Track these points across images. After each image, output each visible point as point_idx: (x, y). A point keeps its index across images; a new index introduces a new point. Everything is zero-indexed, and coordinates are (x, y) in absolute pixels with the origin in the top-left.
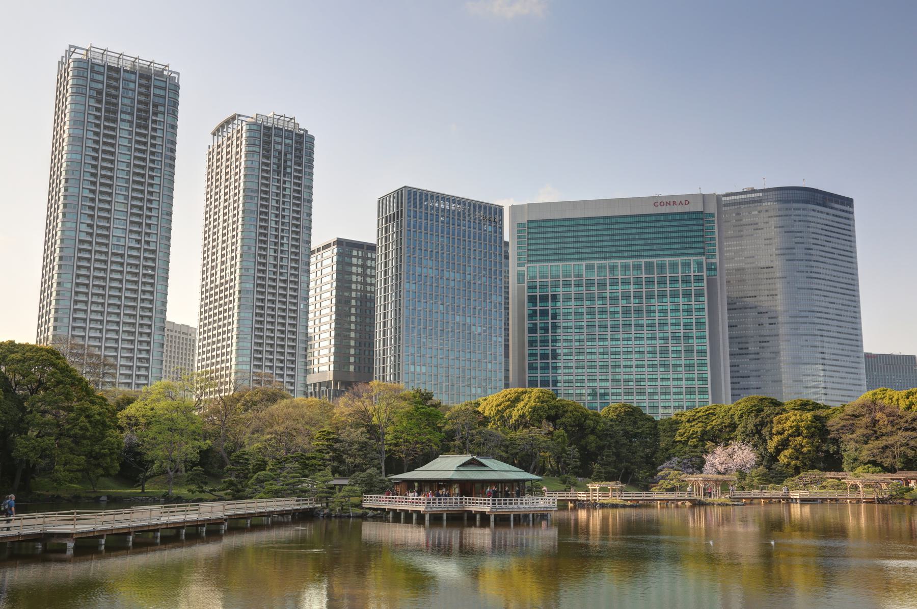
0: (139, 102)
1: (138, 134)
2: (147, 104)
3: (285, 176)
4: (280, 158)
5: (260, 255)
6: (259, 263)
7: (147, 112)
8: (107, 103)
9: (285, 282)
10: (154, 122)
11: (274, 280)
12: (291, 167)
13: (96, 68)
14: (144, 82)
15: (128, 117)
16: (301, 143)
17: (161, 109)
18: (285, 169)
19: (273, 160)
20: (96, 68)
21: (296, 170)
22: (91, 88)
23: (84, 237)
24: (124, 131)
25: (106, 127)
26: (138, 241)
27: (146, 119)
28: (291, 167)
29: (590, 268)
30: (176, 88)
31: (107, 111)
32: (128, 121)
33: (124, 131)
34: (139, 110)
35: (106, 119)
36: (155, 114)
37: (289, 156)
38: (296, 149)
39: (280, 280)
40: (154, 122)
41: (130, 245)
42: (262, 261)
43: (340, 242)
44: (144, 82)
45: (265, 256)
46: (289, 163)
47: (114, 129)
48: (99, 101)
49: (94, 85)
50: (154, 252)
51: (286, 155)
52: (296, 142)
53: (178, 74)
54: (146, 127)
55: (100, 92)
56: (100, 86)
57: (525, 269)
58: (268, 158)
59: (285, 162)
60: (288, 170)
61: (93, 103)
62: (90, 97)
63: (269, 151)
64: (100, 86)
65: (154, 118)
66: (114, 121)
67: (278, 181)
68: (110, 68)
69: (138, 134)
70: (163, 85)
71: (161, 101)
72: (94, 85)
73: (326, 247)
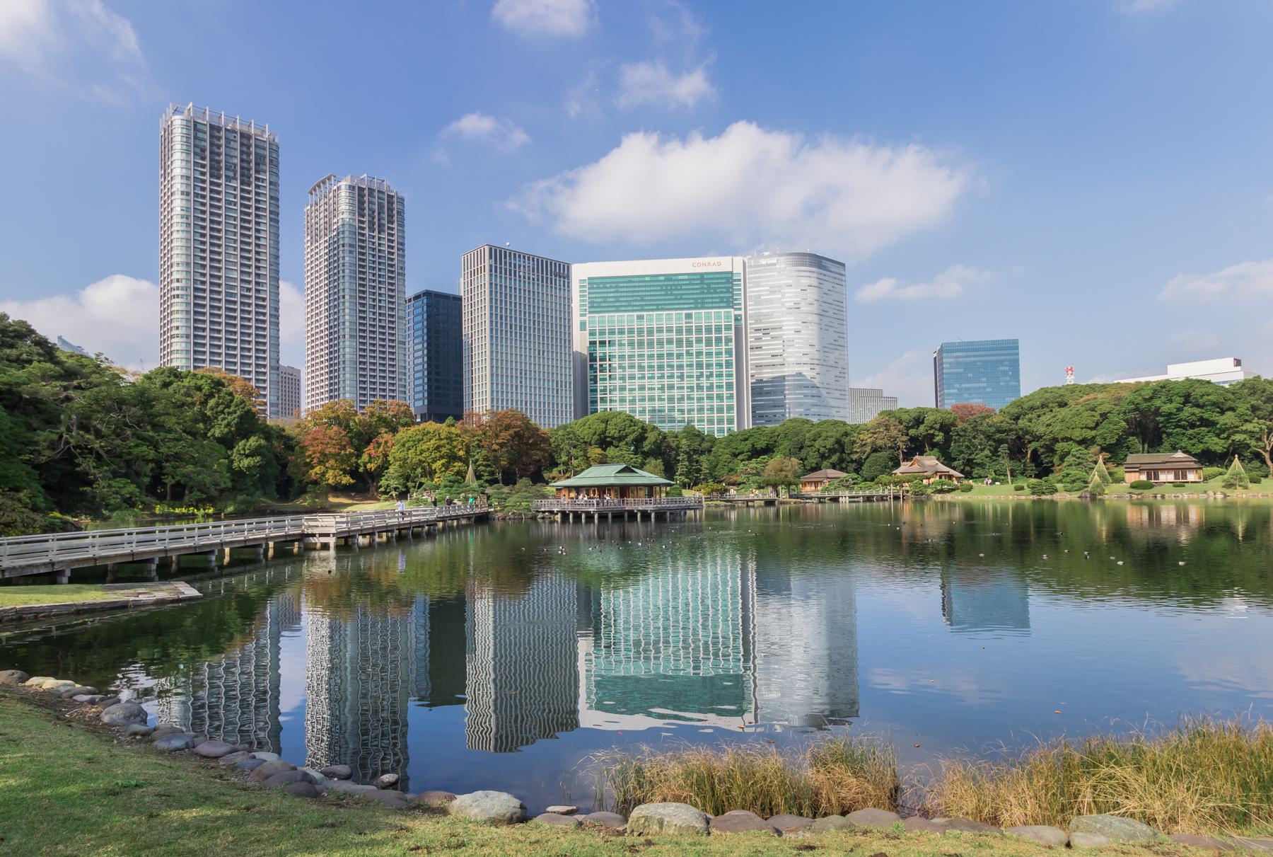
7: (249, 170)
8: (211, 160)
9: (383, 327)
11: (374, 326)
19: (366, 219)
20: (199, 127)
24: (230, 188)
30: (274, 148)
31: (211, 168)
40: (257, 179)
43: (428, 294)
44: (245, 141)
45: (363, 305)
48: (203, 158)
49: (198, 142)
50: (264, 300)
54: (249, 185)
56: (203, 143)
57: (586, 318)
64: (203, 143)
68: (212, 127)
72: (198, 142)
73: (417, 297)
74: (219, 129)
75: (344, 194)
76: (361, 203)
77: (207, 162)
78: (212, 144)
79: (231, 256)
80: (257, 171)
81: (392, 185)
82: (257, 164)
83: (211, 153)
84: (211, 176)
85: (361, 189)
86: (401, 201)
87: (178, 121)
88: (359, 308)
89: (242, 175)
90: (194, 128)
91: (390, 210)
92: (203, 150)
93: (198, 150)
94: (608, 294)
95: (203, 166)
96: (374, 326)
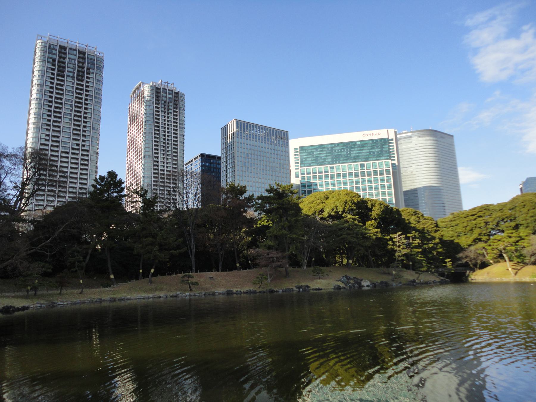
0: (79, 67)
1: (77, 84)
2: (83, 68)
3: (168, 114)
4: (166, 106)
5: (155, 157)
6: (155, 161)
7: (83, 72)
8: (59, 66)
10: (88, 78)
11: (163, 170)
12: (172, 109)
13: (52, 46)
14: (81, 55)
15: (71, 74)
16: (177, 97)
17: (92, 71)
18: (168, 110)
19: (161, 106)
21: (174, 111)
22: (48, 57)
23: (44, 142)
24: (69, 83)
25: (58, 80)
26: (78, 145)
27: (83, 76)
28: (172, 109)
29: (332, 168)
31: (58, 70)
32: (72, 77)
33: (69, 83)
34: (78, 71)
35: (58, 75)
36: (88, 73)
37: (170, 104)
38: (174, 100)
39: (167, 171)
41: (73, 147)
42: (157, 160)
44: (81, 55)
46: (170, 107)
47: (63, 81)
48: (54, 65)
49: (51, 56)
50: (88, 151)
51: (169, 103)
52: (174, 97)
53: (103, 53)
54: (82, 81)
55: (54, 60)
56: (54, 56)
58: (158, 104)
59: (168, 107)
60: (170, 111)
61: (50, 66)
62: (48, 62)
63: (159, 100)
65: (88, 76)
66: (63, 76)
67: (165, 117)
69: (77, 84)
70: (93, 57)
71: (92, 66)
72: (51, 56)
74: (65, 48)
75: (146, 89)
76: (158, 96)
77: (56, 67)
78: (60, 57)
79: (66, 123)
80: (88, 73)
81: (178, 88)
82: (88, 69)
83: (59, 62)
84: (58, 75)
85: (158, 89)
86: (183, 96)
87: (39, 43)
88: (154, 159)
89: (78, 75)
90: (49, 48)
91: (176, 101)
92: (54, 60)
93: (51, 60)
94: (310, 155)
95: (53, 70)
96: (163, 170)
